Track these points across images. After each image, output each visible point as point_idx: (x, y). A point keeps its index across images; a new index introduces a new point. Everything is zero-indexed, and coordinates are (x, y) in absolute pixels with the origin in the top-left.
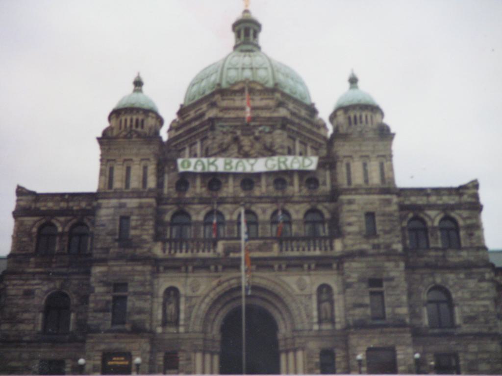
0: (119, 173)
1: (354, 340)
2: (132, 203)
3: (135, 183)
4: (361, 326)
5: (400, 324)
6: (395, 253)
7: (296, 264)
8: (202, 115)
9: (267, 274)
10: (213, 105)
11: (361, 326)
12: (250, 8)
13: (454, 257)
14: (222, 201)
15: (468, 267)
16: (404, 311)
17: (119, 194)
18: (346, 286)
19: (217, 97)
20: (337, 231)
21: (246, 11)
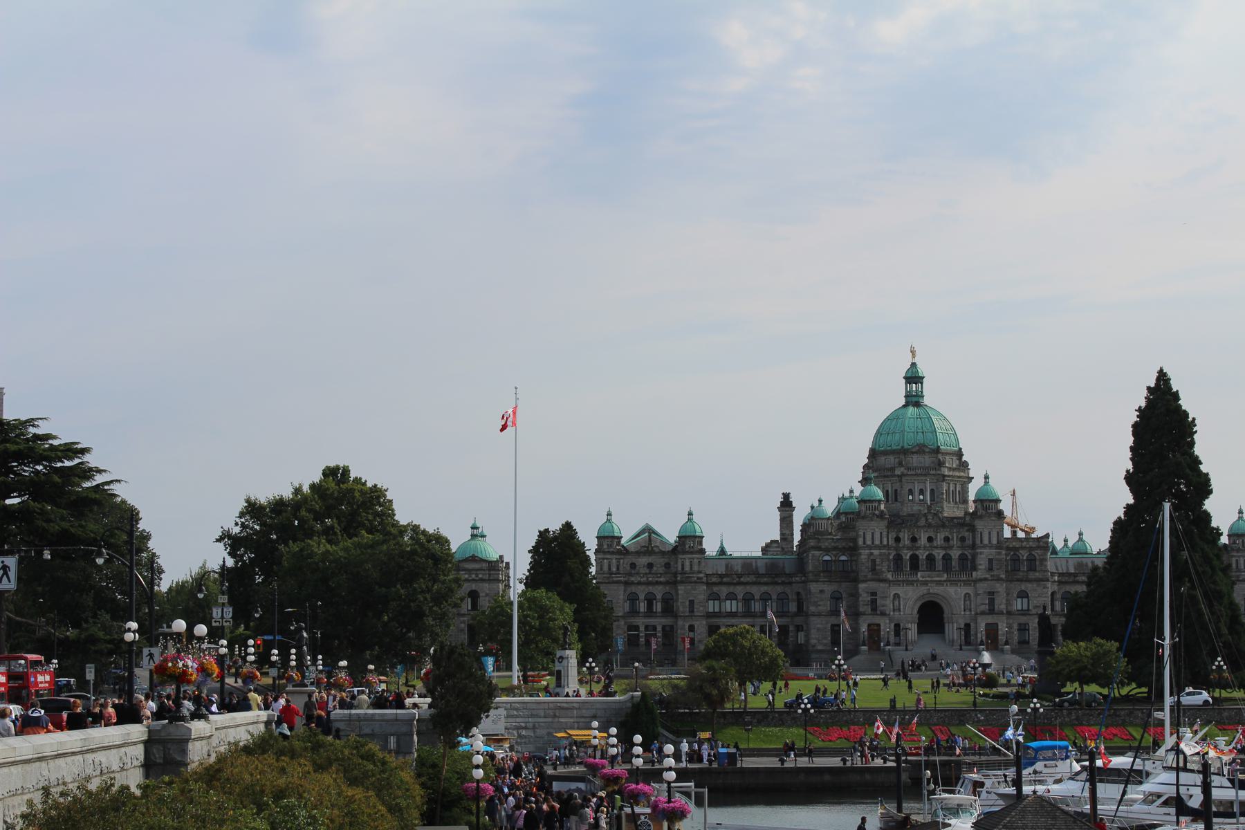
0: (869, 537)
1: (980, 619)
2: (876, 552)
3: (877, 542)
4: (983, 613)
5: (1002, 613)
6: (1001, 579)
7: (954, 583)
8: (893, 469)
9: (941, 588)
10: (900, 464)
11: (983, 613)
12: (916, 361)
13: (1032, 575)
14: (918, 548)
15: (1039, 580)
16: (1003, 607)
17: (870, 548)
18: (977, 595)
19: (902, 457)
20: (974, 568)
21: (913, 364)
